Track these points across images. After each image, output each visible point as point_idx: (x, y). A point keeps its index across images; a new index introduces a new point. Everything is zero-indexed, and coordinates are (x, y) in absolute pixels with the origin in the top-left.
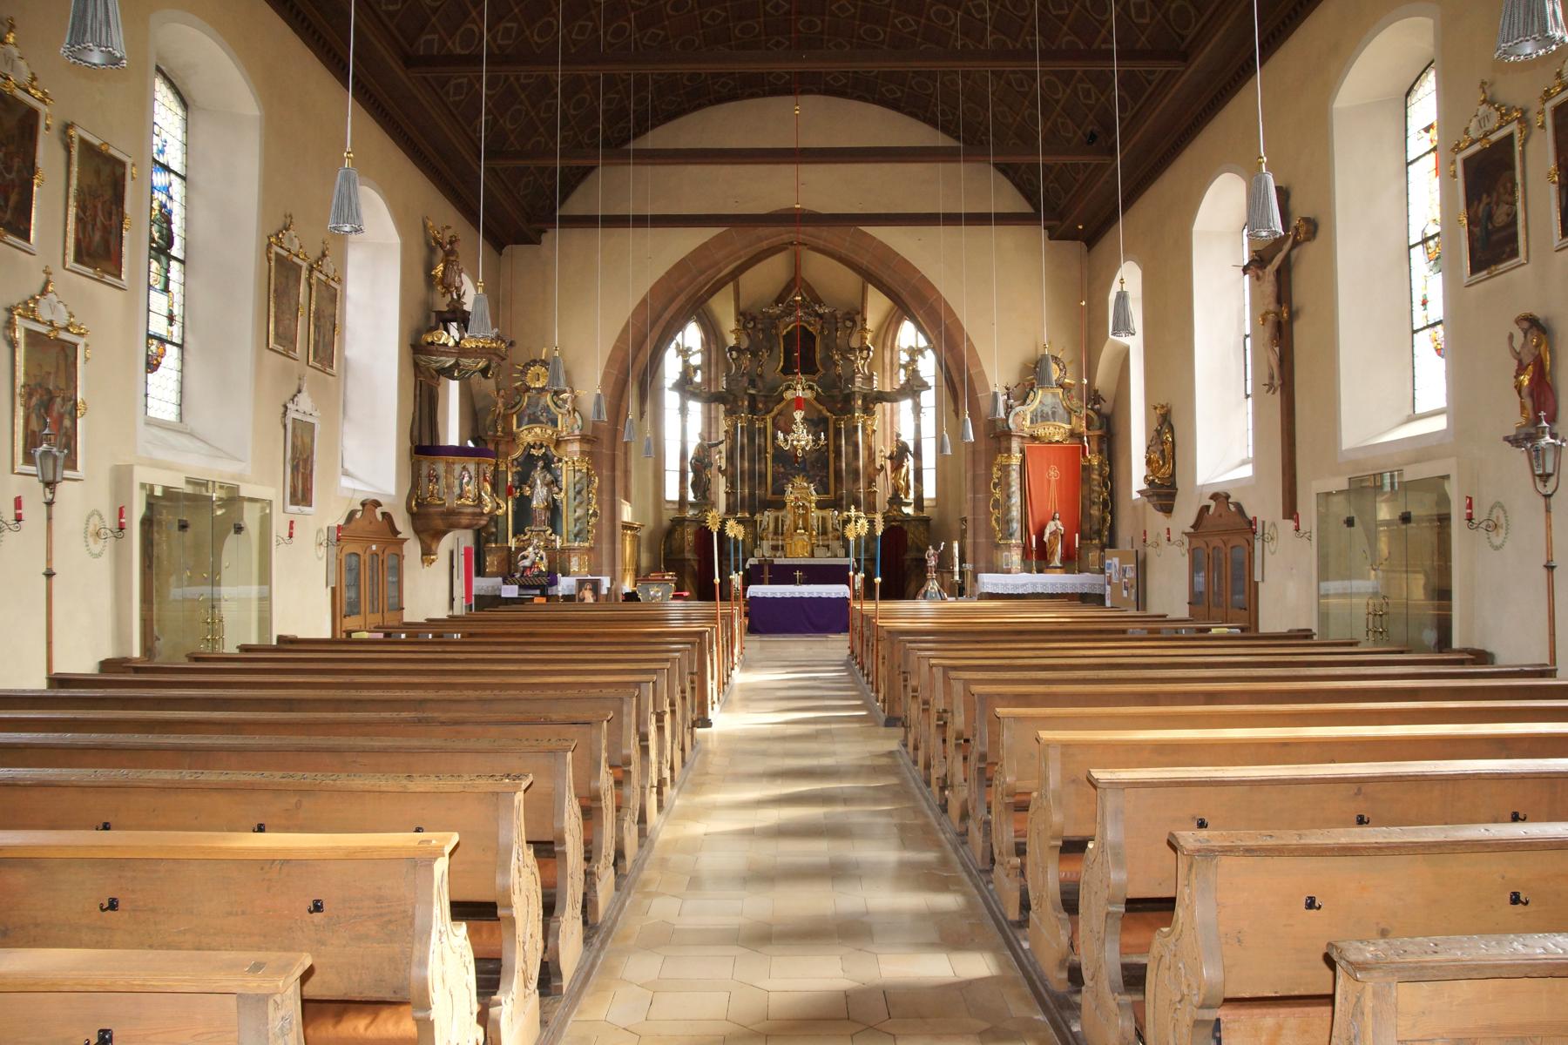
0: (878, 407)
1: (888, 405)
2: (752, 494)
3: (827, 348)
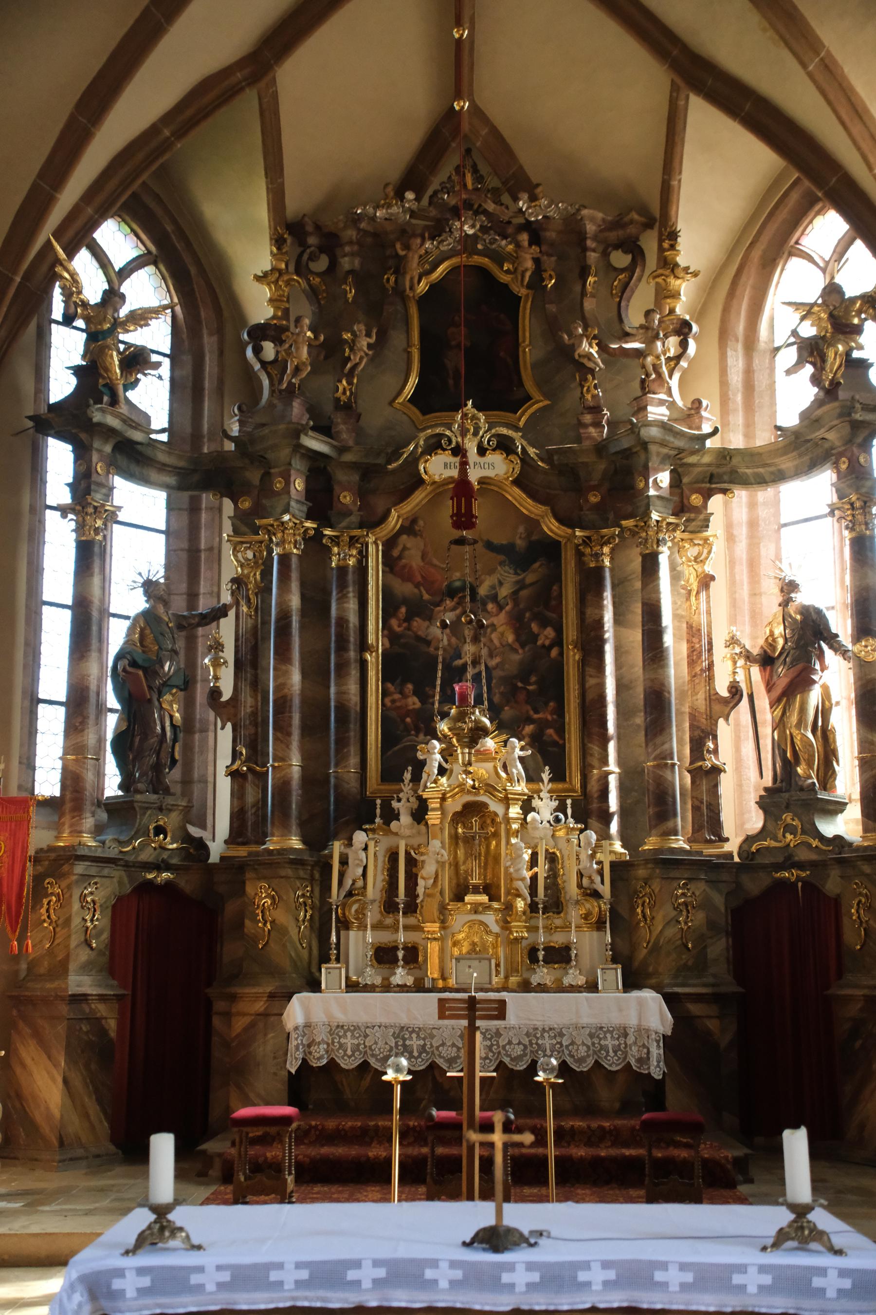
0: (716, 503)
1: (741, 495)
2: (315, 780)
3: (553, 328)
